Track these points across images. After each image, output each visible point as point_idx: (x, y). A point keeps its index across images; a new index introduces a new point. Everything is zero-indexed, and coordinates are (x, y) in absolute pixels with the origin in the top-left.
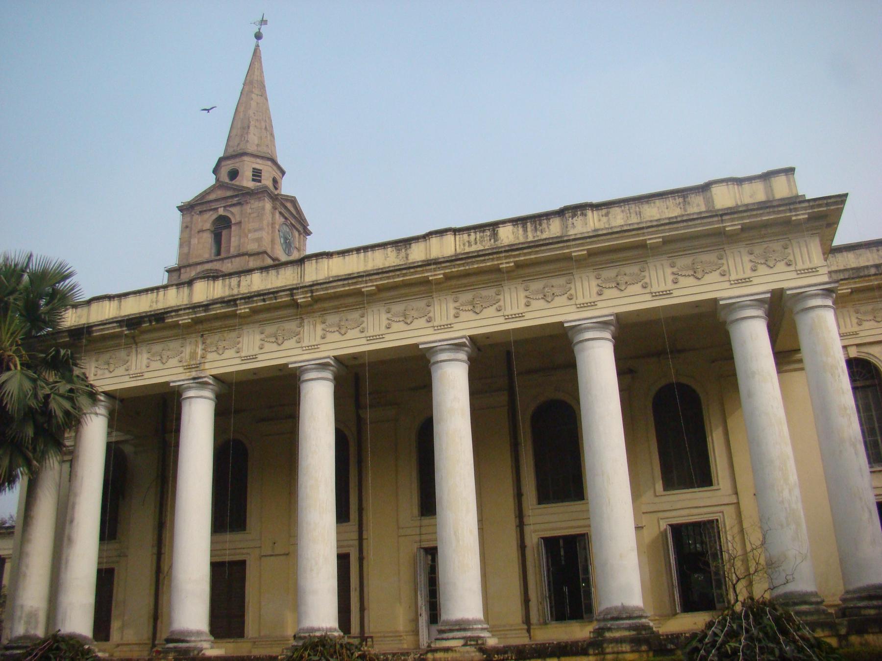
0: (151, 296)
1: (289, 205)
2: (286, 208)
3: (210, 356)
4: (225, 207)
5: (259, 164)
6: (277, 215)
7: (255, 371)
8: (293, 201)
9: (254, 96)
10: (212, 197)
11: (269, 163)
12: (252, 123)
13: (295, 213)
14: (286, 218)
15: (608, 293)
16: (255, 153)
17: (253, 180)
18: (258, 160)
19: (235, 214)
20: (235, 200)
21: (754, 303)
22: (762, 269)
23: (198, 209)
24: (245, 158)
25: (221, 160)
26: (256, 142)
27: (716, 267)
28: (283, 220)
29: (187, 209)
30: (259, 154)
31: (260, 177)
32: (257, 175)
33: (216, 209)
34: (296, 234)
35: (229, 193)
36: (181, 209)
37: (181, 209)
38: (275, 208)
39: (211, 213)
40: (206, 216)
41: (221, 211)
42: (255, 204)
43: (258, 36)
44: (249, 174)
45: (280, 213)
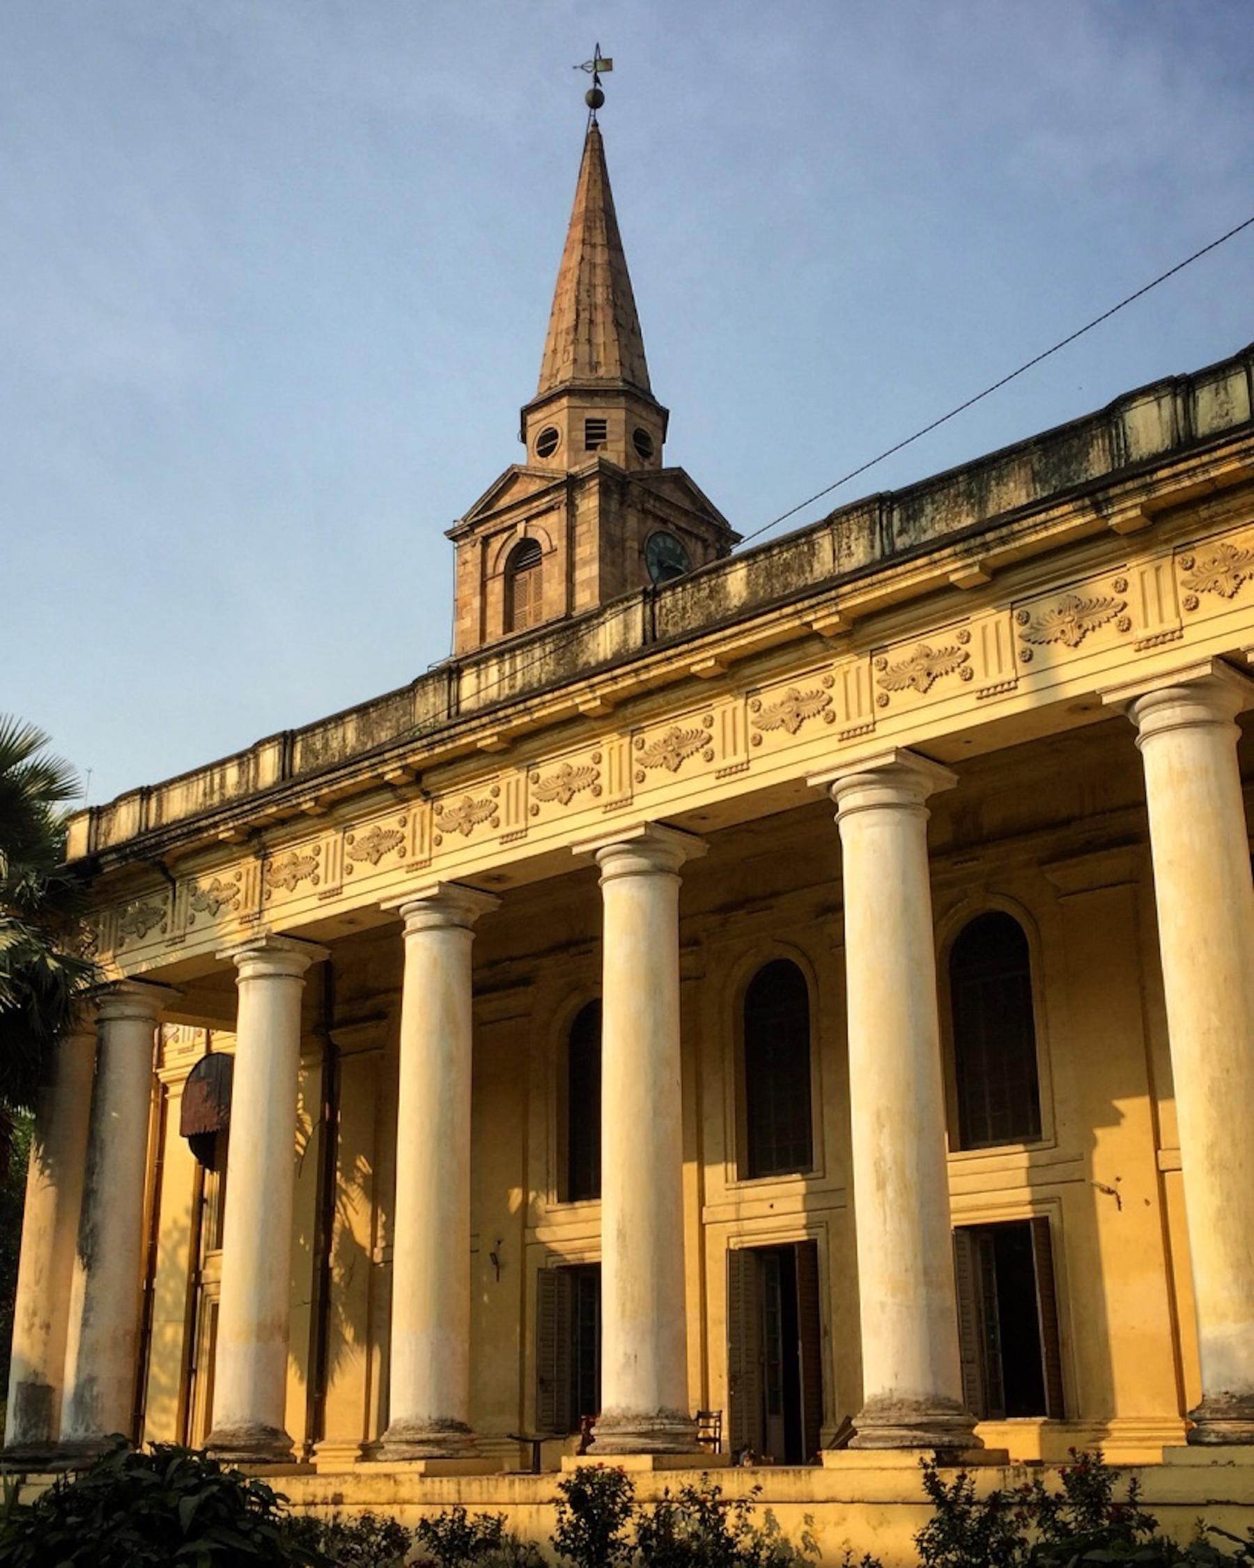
0: (200, 786)
1: (667, 491)
2: (658, 498)
3: (279, 894)
4: (528, 520)
6: (632, 521)
7: (349, 918)
8: (679, 477)
10: (505, 502)
11: (622, 400)
12: (585, 315)
13: (687, 505)
14: (664, 521)
15: (899, 699)
16: (593, 385)
17: (590, 447)
18: (597, 399)
19: (548, 531)
21: (1175, 691)
22: (1210, 603)
23: (481, 531)
25: (526, 411)
27: (1111, 612)
28: (652, 526)
29: (465, 535)
30: (603, 385)
31: (604, 436)
32: (595, 434)
33: (514, 526)
34: (697, 548)
35: (535, 487)
36: (454, 536)
37: (454, 536)
38: (622, 503)
39: (505, 535)
40: (496, 544)
43: (596, 100)
44: (581, 436)
45: (645, 511)
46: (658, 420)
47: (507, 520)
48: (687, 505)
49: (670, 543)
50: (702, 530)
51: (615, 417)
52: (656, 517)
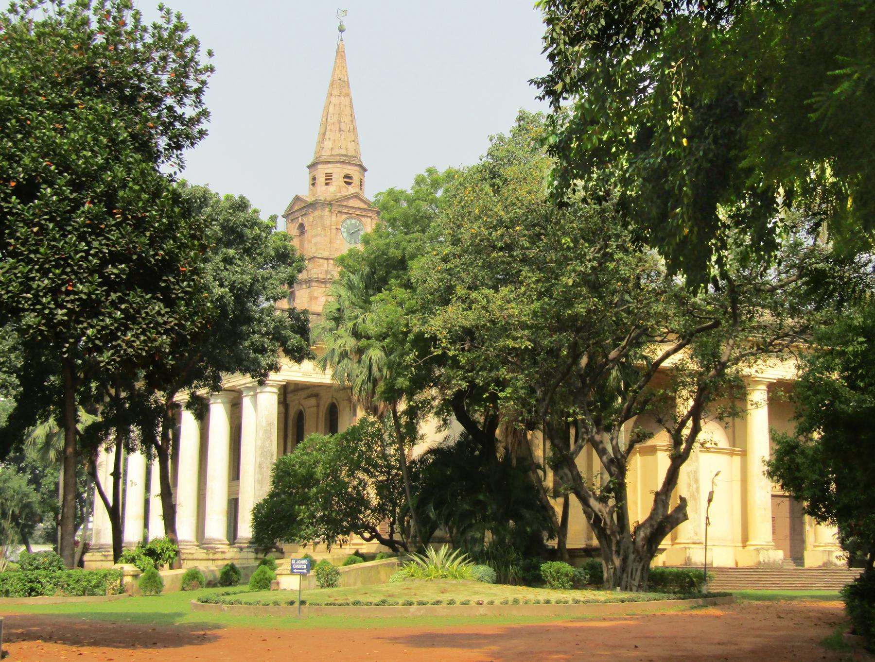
2: (346, 206)
5: (329, 169)
6: (334, 218)
9: (333, 99)
10: (296, 208)
13: (362, 205)
17: (327, 184)
19: (307, 221)
20: (304, 211)
24: (320, 166)
26: (330, 147)
32: (329, 178)
41: (300, 221)
42: (317, 213)
43: (342, 30)
44: (323, 180)
46: (357, 168)
47: (297, 214)
48: (362, 205)
49: (353, 221)
50: (369, 214)
51: (338, 172)
52: (346, 213)
